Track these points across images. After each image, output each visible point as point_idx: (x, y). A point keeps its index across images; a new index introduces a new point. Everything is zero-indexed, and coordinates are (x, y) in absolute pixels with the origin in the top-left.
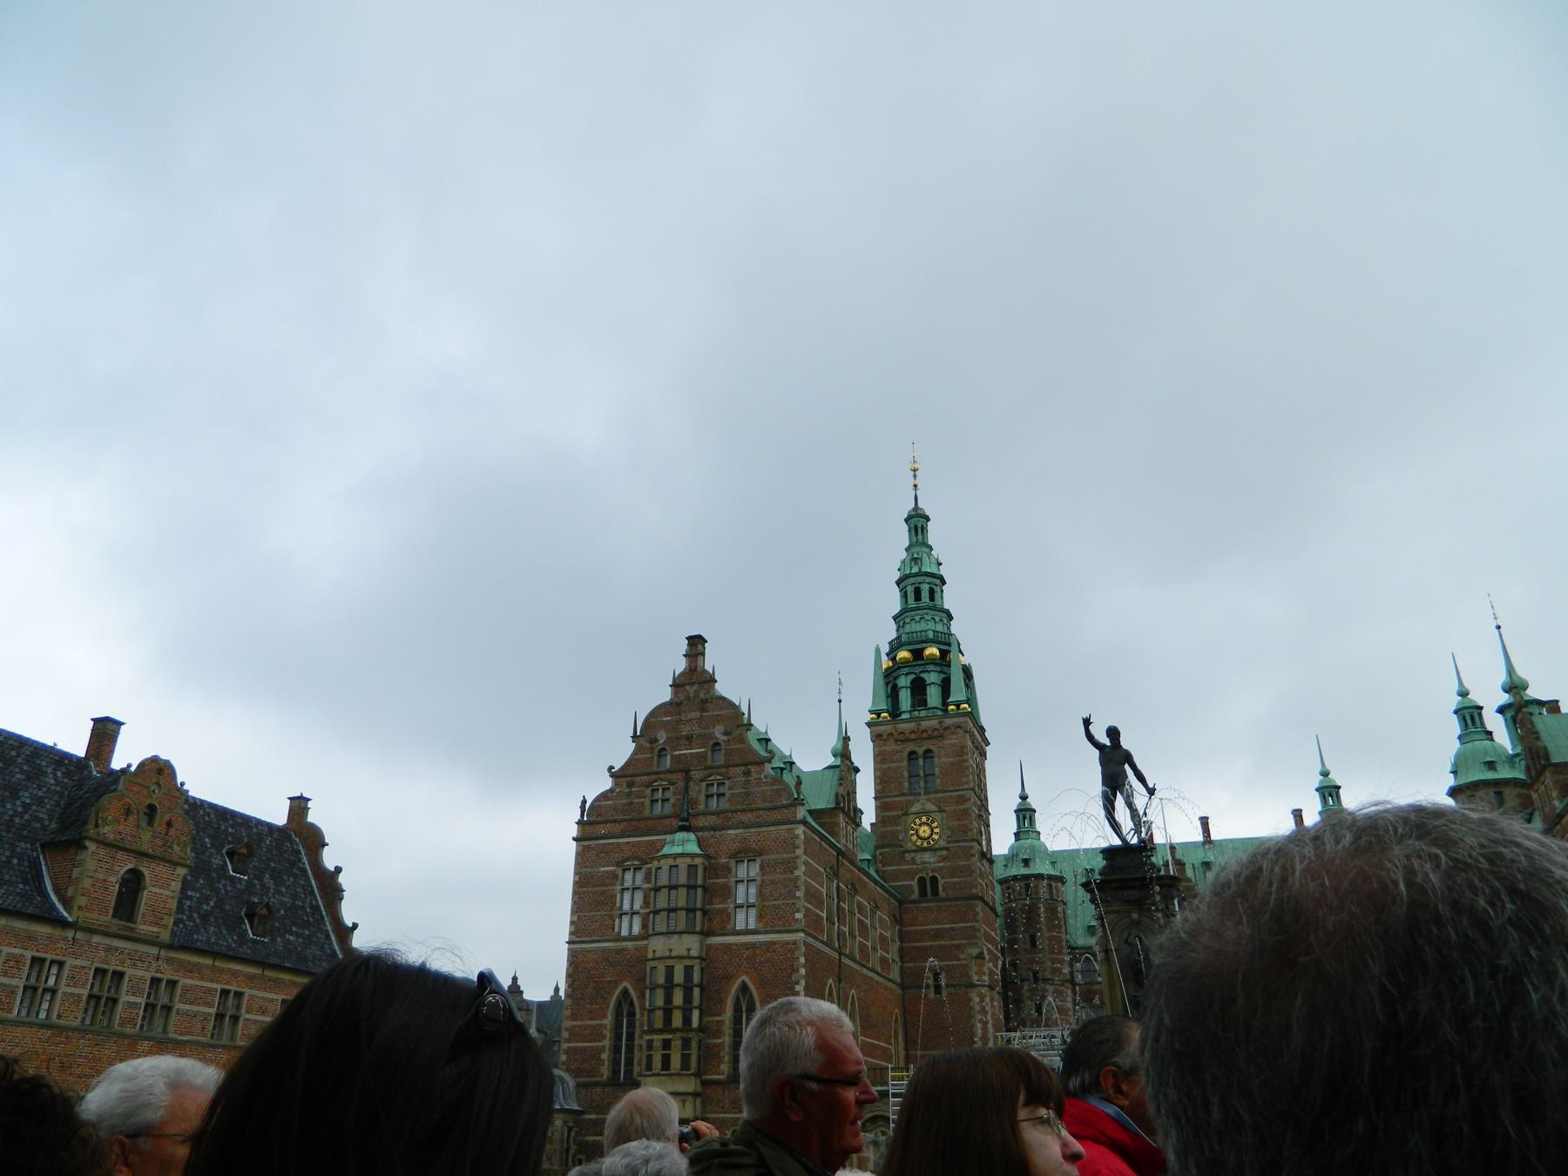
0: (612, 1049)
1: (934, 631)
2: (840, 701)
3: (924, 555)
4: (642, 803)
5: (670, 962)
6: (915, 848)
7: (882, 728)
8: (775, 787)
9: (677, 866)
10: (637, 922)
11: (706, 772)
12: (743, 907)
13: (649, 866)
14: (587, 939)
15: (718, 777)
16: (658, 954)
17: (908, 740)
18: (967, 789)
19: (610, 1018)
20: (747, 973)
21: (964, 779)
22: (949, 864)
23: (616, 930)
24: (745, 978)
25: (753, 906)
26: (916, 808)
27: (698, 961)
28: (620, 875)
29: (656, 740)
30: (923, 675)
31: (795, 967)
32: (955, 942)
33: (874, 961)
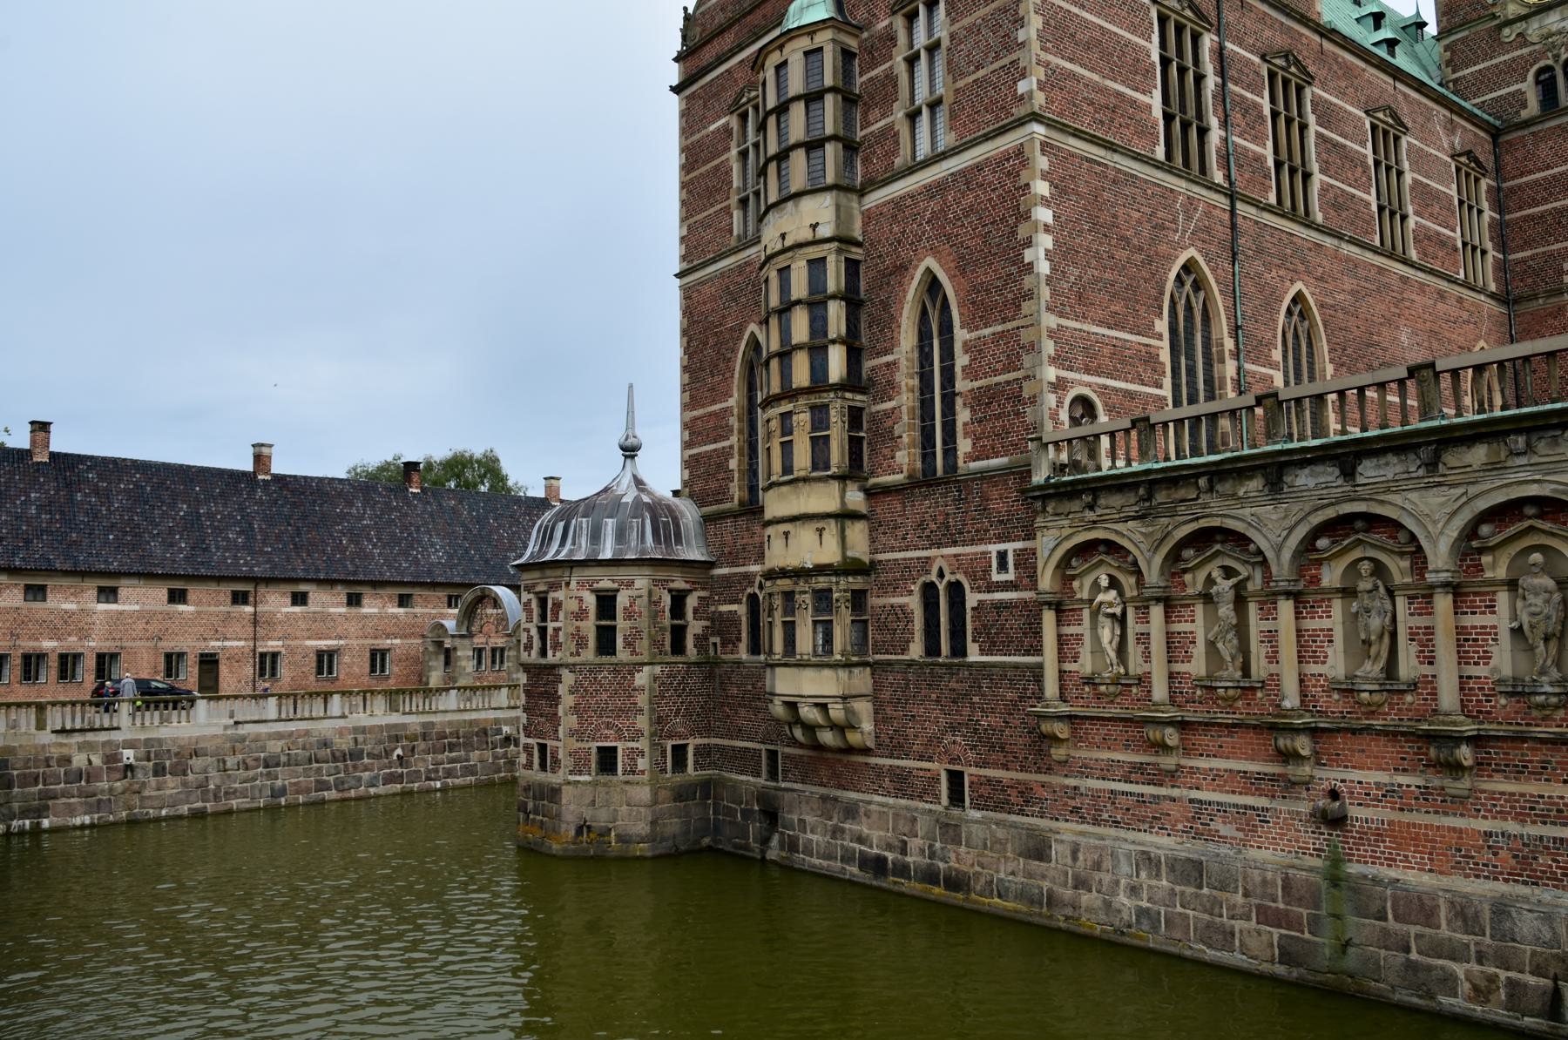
6: (1524, 11)
16: (769, 252)
19: (736, 395)
20: (934, 251)
24: (930, 262)
27: (835, 245)
31: (1022, 208)
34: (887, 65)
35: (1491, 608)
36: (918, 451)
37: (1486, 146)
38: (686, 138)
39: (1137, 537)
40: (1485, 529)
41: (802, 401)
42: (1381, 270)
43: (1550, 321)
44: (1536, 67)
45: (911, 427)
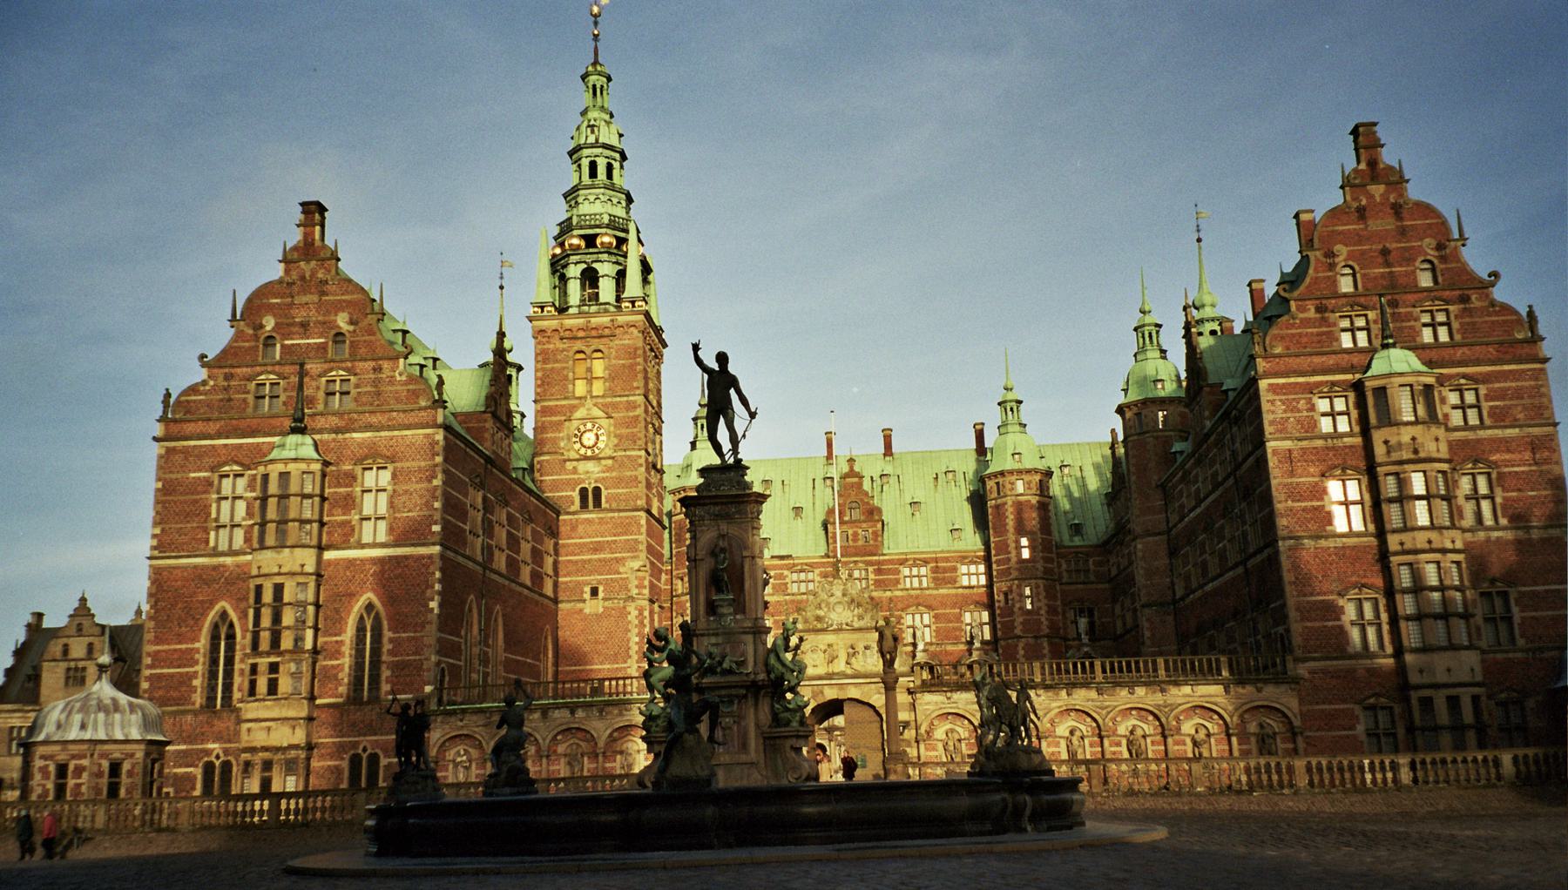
0: (206, 676)
1: (610, 215)
2: (502, 287)
3: (603, 123)
4: (244, 400)
5: (278, 580)
6: (578, 457)
8: (411, 387)
9: (289, 473)
10: (239, 535)
11: (326, 366)
12: (370, 519)
13: (254, 472)
14: (174, 554)
15: (341, 373)
17: (575, 338)
21: (635, 384)
22: (614, 474)
23: (212, 543)
25: (383, 518)
26: (581, 413)
28: (216, 482)
29: (262, 326)
30: (594, 265)
33: (525, 576)
34: (349, 489)
35: (615, 761)
36: (352, 687)
38: (164, 473)
39: (484, 734)
40: (615, 734)
41: (287, 657)
42: (520, 594)
43: (576, 616)
45: (350, 675)
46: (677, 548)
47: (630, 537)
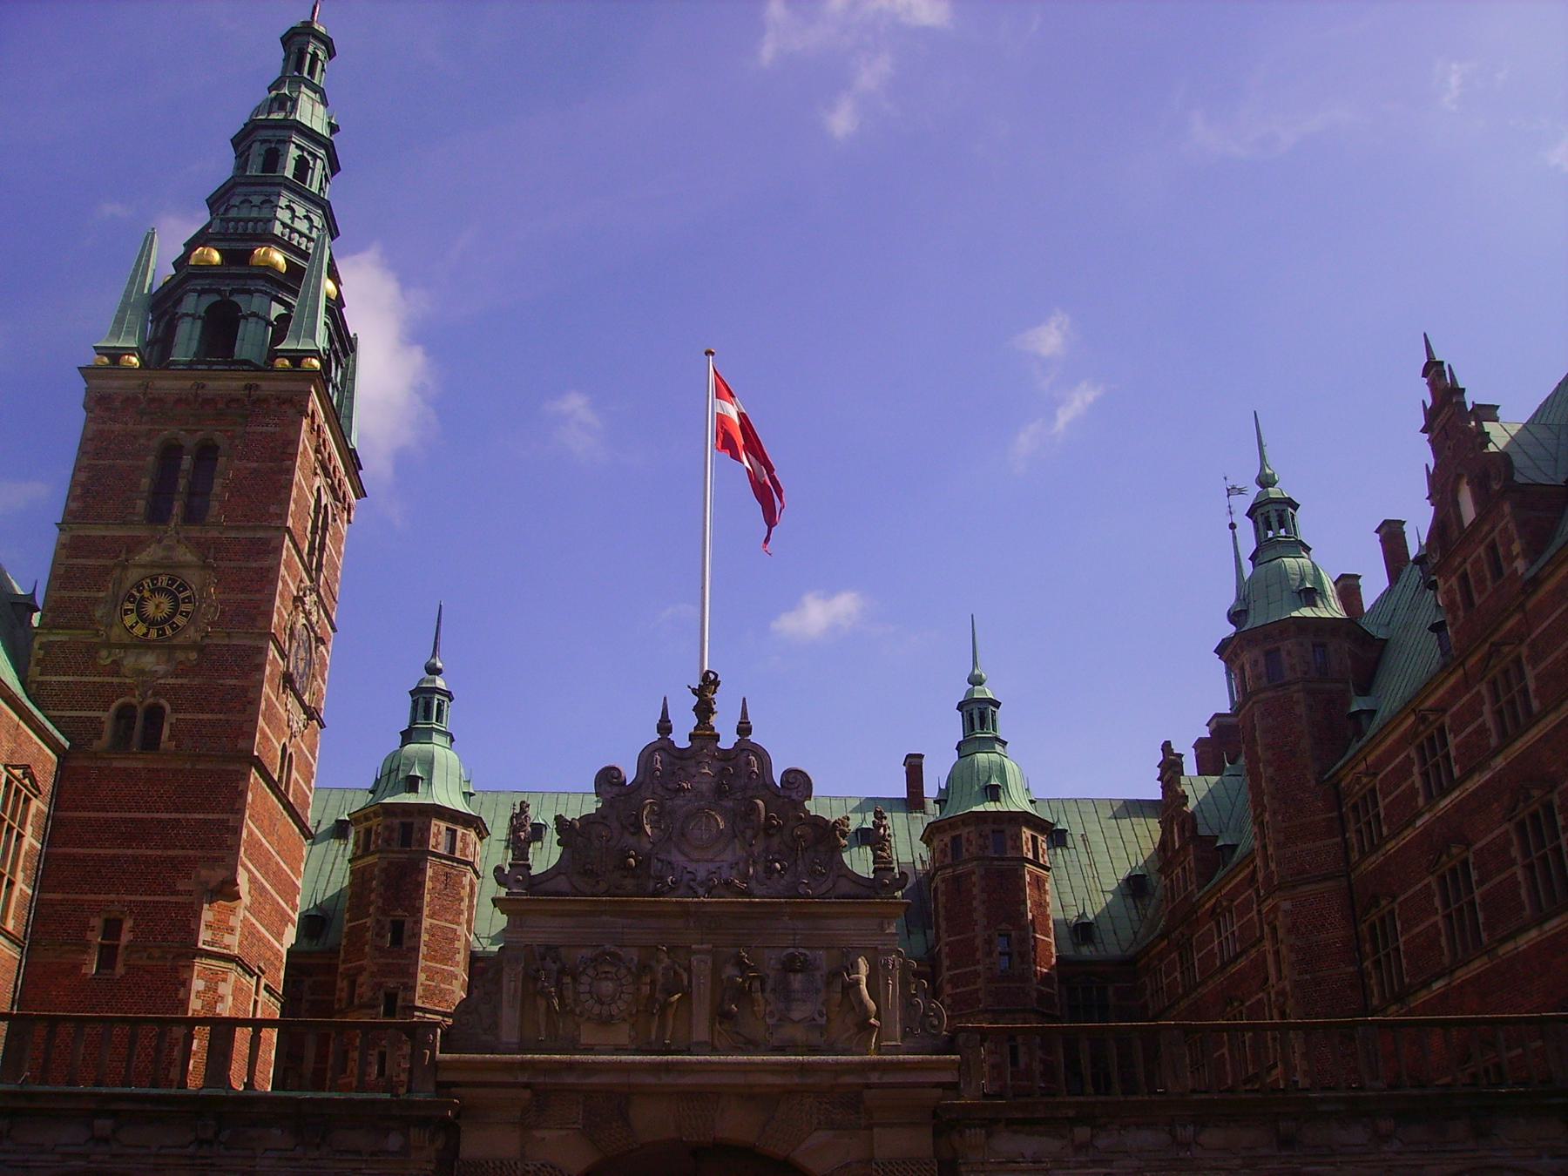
1: (284, 225)
6: (126, 639)
7: (116, 384)
18: (278, 528)
21: (272, 509)
30: (235, 298)
32: (170, 853)
37: (49, 766)
44: (121, 700)
46: (350, 921)
47: (216, 816)
